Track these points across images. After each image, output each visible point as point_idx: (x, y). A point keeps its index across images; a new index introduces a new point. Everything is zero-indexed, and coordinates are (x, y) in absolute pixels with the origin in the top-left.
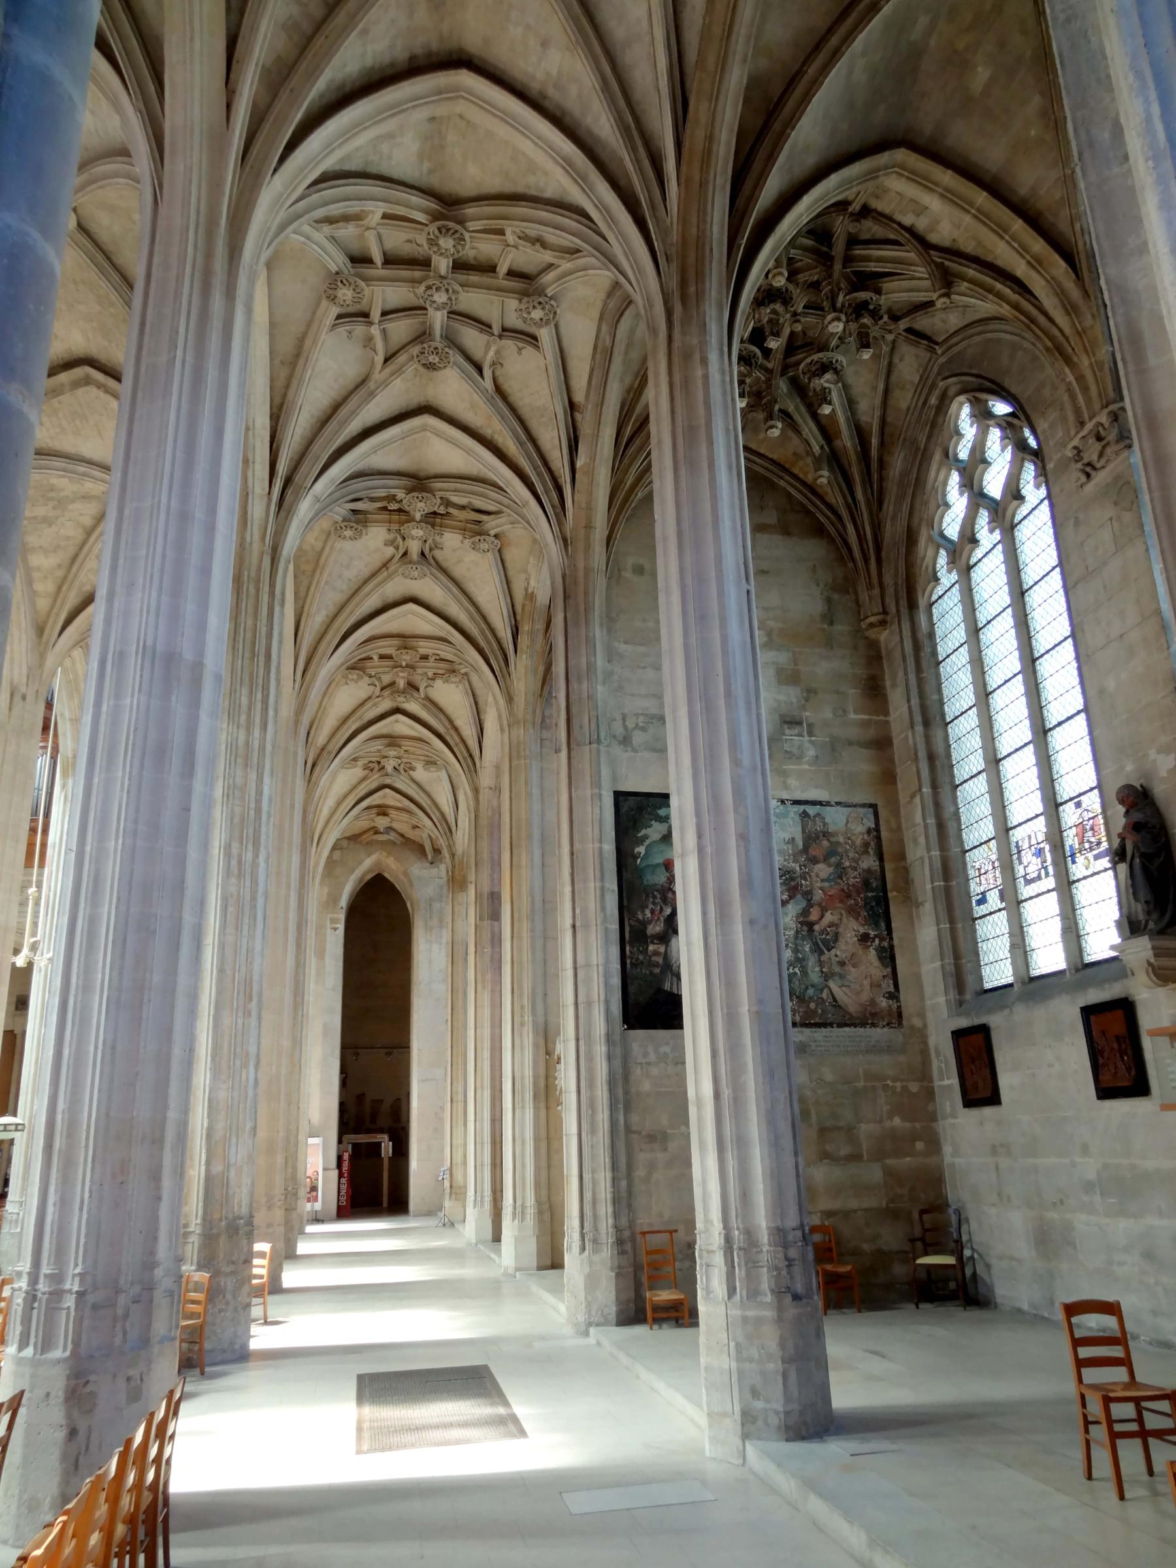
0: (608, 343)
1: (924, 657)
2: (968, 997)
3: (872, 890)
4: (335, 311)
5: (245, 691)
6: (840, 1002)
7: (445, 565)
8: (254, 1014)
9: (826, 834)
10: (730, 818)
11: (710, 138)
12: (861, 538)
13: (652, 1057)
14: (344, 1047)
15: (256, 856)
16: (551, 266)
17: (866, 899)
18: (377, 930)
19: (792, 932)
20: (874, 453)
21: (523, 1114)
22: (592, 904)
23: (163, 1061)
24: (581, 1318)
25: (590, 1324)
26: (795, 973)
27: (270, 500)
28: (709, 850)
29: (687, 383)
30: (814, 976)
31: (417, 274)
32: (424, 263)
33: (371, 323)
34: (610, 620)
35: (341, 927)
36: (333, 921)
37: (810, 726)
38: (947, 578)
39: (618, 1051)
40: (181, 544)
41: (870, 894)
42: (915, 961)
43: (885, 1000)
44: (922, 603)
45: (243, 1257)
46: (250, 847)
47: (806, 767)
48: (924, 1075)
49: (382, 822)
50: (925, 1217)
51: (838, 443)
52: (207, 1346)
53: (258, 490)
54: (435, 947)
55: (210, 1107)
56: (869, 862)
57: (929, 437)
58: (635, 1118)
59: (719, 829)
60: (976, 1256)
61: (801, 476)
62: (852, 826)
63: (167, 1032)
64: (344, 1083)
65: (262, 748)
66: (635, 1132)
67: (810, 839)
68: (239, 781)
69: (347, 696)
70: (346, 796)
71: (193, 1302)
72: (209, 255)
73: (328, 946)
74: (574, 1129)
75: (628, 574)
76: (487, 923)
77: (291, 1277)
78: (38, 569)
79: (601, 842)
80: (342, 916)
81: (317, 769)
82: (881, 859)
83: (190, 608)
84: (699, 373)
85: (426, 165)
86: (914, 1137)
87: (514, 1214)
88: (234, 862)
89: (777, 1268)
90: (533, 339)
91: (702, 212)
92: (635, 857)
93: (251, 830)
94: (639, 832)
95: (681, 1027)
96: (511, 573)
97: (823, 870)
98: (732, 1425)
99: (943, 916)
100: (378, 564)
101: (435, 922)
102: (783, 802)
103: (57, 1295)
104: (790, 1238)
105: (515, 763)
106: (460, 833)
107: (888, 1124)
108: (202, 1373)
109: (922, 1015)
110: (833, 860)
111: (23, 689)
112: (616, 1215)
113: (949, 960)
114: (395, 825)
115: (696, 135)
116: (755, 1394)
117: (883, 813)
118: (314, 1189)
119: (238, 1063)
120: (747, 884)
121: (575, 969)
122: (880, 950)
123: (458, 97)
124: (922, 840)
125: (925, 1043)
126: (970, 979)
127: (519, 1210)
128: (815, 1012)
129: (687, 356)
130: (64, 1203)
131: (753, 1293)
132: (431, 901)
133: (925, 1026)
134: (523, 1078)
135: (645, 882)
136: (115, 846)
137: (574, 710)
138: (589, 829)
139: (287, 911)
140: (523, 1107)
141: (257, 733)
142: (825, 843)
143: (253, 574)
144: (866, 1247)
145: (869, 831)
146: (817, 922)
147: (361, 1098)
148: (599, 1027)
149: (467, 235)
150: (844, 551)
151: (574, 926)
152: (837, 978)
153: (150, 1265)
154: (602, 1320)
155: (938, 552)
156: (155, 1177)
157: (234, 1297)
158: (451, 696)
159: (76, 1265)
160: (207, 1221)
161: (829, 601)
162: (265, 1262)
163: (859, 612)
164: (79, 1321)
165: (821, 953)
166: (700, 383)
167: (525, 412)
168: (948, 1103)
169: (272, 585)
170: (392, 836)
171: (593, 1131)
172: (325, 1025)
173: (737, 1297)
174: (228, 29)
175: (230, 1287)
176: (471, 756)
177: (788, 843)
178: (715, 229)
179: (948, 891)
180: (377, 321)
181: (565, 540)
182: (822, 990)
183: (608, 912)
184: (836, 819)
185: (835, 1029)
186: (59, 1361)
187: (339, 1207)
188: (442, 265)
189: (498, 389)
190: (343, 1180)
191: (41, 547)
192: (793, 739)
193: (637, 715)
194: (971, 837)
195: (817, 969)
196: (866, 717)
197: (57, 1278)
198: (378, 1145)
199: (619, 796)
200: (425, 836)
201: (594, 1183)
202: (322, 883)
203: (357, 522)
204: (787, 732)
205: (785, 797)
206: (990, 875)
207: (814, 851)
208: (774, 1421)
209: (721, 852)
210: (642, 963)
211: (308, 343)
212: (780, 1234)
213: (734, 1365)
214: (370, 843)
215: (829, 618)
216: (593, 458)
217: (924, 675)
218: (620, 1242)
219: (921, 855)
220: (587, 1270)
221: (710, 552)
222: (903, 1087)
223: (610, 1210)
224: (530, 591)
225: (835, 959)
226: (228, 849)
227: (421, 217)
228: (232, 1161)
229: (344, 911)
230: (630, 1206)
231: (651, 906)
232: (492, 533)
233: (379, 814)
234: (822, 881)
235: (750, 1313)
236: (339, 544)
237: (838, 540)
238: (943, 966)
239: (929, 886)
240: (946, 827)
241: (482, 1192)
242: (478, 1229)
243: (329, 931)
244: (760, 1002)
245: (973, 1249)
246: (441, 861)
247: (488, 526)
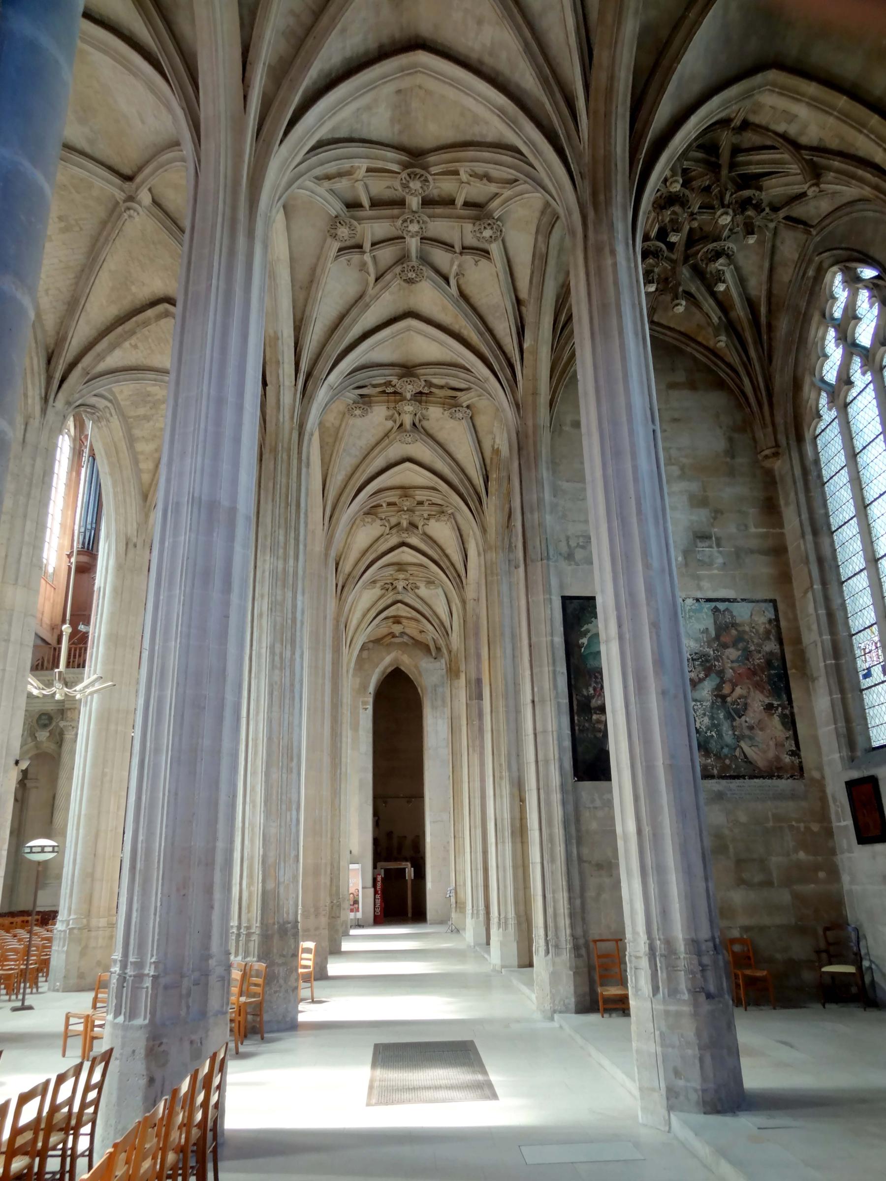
0: (544, 250)
1: (811, 479)
2: (859, 753)
3: (774, 669)
4: (336, 245)
5: (282, 532)
6: (750, 759)
7: (431, 432)
8: (295, 771)
9: (734, 625)
10: (644, 611)
11: (612, 78)
12: (756, 388)
13: (598, 803)
14: (376, 798)
15: (293, 653)
16: (496, 195)
17: (769, 677)
18: (397, 710)
19: (708, 704)
20: (763, 320)
21: (504, 845)
22: (547, 685)
23: (213, 803)
24: (548, 1006)
25: (555, 1012)
26: (712, 736)
27: (296, 390)
28: (627, 636)
29: (600, 270)
30: (728, 738)
31: (396, 212)
32: (400, 203)
33: (364, 252)
34: (554, 465)
35: (370, 707)
37: (718, 540)
38: (828, 415)
39: (571, 798)
40: (218, 422)
41: (772, 672)
42: (813, 724)
43: (788, 757)
44: (808, 437)
45: (291, 952)
46: (289, 647)
47: (716, 572)
48: (823, 815)
49: (397, 629)
50: (828, 933)
51: (733, 314)
52: (266, 1017)
53: (287, 383)
54: (440, 722)
55: (264, 840)
56: (771, 646)
57: (809, 302)
58: (585, 851)
59: (635, 618)
60: (873, 966)
61: (704, 342)
62: (756, 618)
64: (377, 824)
65: (295, 573)
66: (585, 862)
67: (721, 629)
68: (279, 598)
69: (365, 535)
70: (369, 610)
71: (256, 985)
72: (234, 208)
73: (361, 722)
74: (538, 859)
75: (567, 428)
76: (475, 702)
77: (335, 968)
78: (142, 453)
79: (552, 635)
80: (370, 700)
81: (346, 589)
82: (781, 642)
83: (225, 467)
84: (609, 262)
85: (397, 128)
86: (817, 868)
87: (499, 924)
88: (277, 658)
89: (692, 972)
90: (486, 253)
91: (608, 135)
92: (580, 647)
93: (289, 634)
94: (582, 627)
95: (608, 778)
96: (481, 435)
97: (733, 653)
98: (659, 1099)
99: (835, 688)
100: (381, 434)
101: (439, 702)
102: (698, 600)
103: (140, 977)
104: (704, 947)
105: (489, 578)
107: (794, 857)
108: (262, 1038)
109: (820, 768)
110: (741, 645)
111: (135, 540)
112: (572, 926)
113: (841, 724)
114: (408, 631)
115: (600, 77)
116: (677, 1073)
117: (780, 606)
118: (356, 902)
119: (284, 807)
120: (659, 662)
121: (535, 735)
122: (783, 717)
123: (416, 72)
124: (815, 627)
125: (823, 791)
126: (860, 740)
127: (502, 921)
128: (729, 767)
129: (599, 250)
130: (144, 909)
131: (673, 992)
132: (436, 686)
133: (823, 777)
134: (502, 820)
135: (588, 666)
136: (174, 646)
137: (528, 535)
138: (543, 626)
139: (323, 695)
140: (503, 842)
141: (291, 562)
142: (734, 632)
143: (285, 445)
144: (778, 956)
145: (770, 621)
146: (729, 695)
148: (555, 779)
149: (430, 178)
150: (742, 400)
151: (533, 702)
152: (747, 739)
154: (563, 1008)
155: (819, 395)
156: (209, 890)
157: (285, 982)
158: (442, 531)
159: (152, 956)
160: (264, 925)
161: (731, 440)
162: (311, 956)
163: (756, 447)
164: (154, 997)
165: (734, 720)
166: (610, 270)
167: (483, 310)
168: (845, 841)
169: (300, 453)
170: (405, 639)
171: (553, 860)
173: (660, 995)
174: (242, 43)
175: (282, 974)
176: (459, 576)
177: (703, 632)
178: (619, 150)
179: (838, 668)
180: (368, 250)
181: (517, 406)
182: (735, 749)
183: (560, 690)
184: (742, 613)
185: (747, 781)
186: (141, 1027)
187: (375, 917)
188: (414, 202)
189: (463, 295)
190: (378, 896)
191: (143, 437)
192: (705, 550)
193: (578, 537)
194: (856, 624)
195: (730, 732)
196: (765, 530)
197: (139, 965)
199: (566, 600)
200: (429, 638)
201: (555, 901)
202: (354, 675)
203: (364, 403)
204: (699, 544)
205: (699, 595)
206: (874, 654)
207: (724, 639)
208: (694, 1097)
209: (637, 637)
210: (588, 729)
211: (318, 271)
212: (694, 944)
213: (659, 1049)
214: (390, 645)
215: (731, 453)
216: (536, 340)
217: (812, 494)
218: (576, 948)
219: (814, 639)
220: (551, 969)
221: (622, 400)
222: (805, 827)
223: (568, 922)
224: (496, 447)
225: (745, 725)
226: (272, 648)
227: (395, 167)
228: (282, 880)
229: (372, 696)
230: (583, 919)
231: (593, 685)
232: (465, 404)
234: (732, 662)
235: (672, 1008)
236: (352, 421)
237: (737, 391)
238: (836, 729)
239: (822, 664)
240: (835, 617)
241: (478, 906)
243: (361, 711)
244: (673, 757)
245: (871, 961)
246: (442, 657)
247: (462, 400)
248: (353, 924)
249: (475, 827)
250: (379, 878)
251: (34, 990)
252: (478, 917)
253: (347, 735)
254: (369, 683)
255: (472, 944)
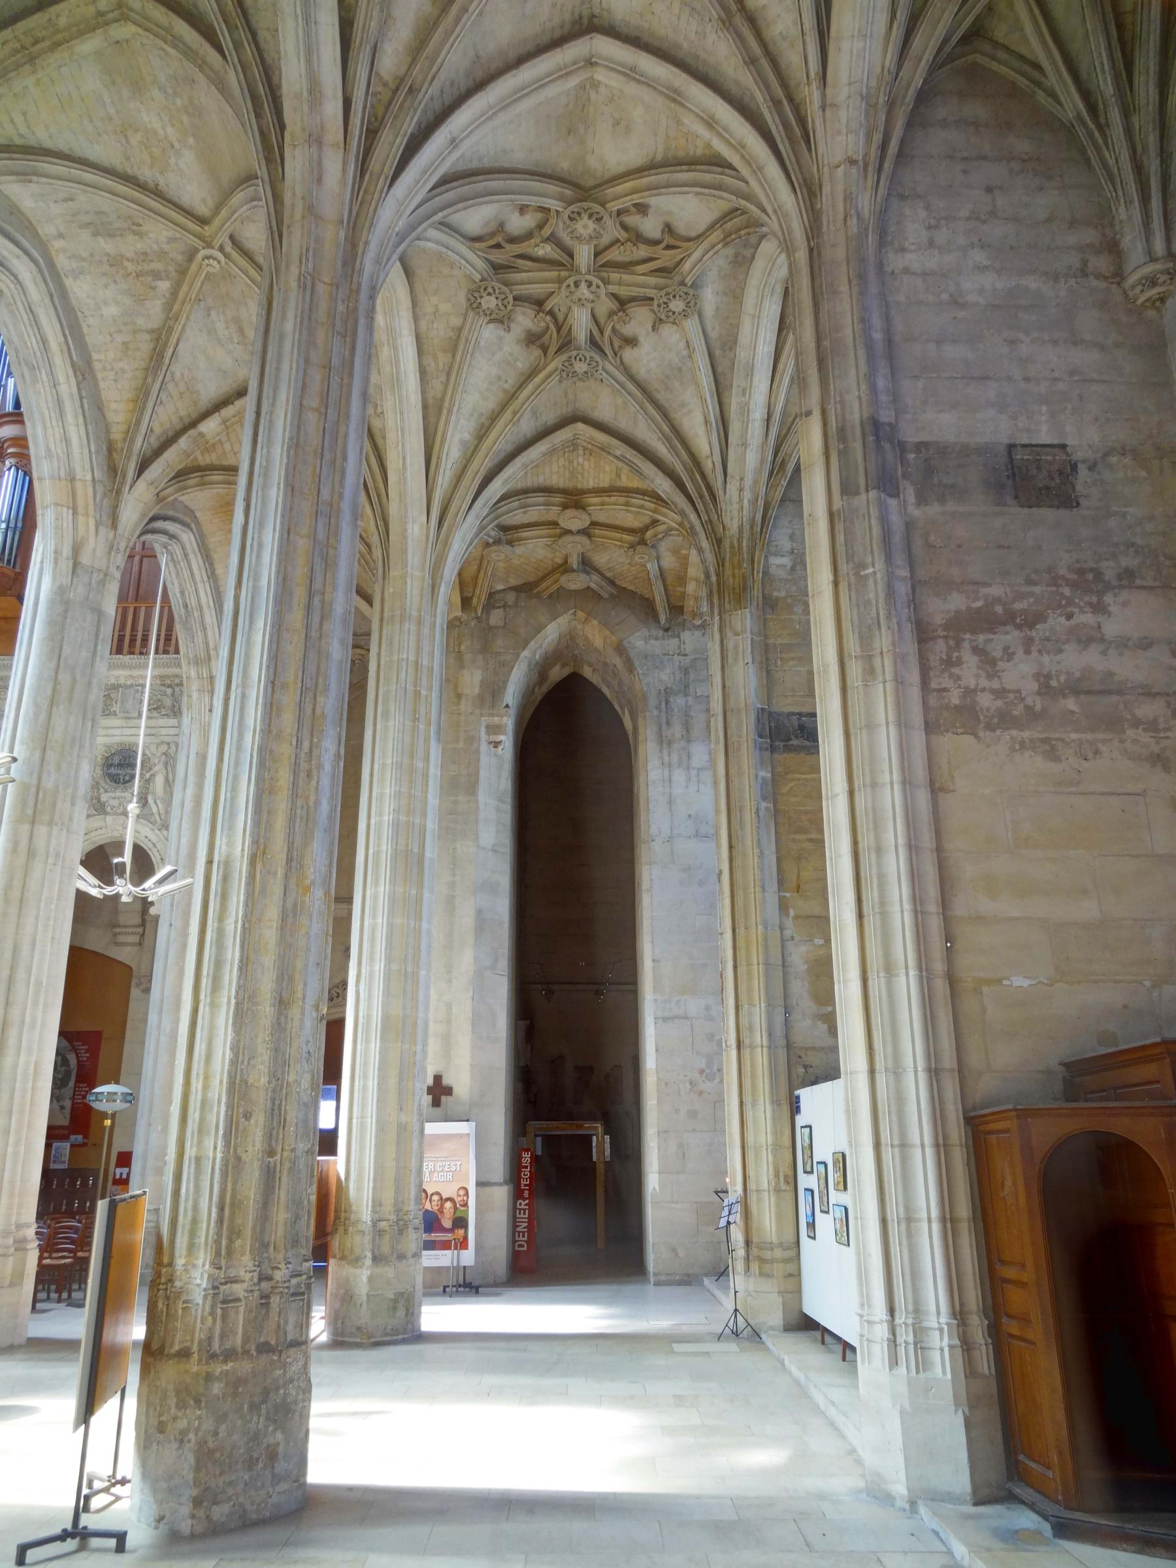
35: (507, 741)
36: (493, 729)
54: (679, 776)
73: (483, 774)
76: (867, 500)
101: (677, 730)
106: (733, 488)
114: (601, 559)
118: (460, 1222)
132: (668, 692)
172: (479, 912)
198: (587, 1139)
229: (512, 712)
233: (565, 507)
241: (918, 1311)
242: (917, 1451)
243: (484, 747)
246: (683, 625)
248: (451, 1281)
249: (889, 969)
251: (65, 1295)
252: (922, 1364)
254: (505, 682)
255: (900, 1489)
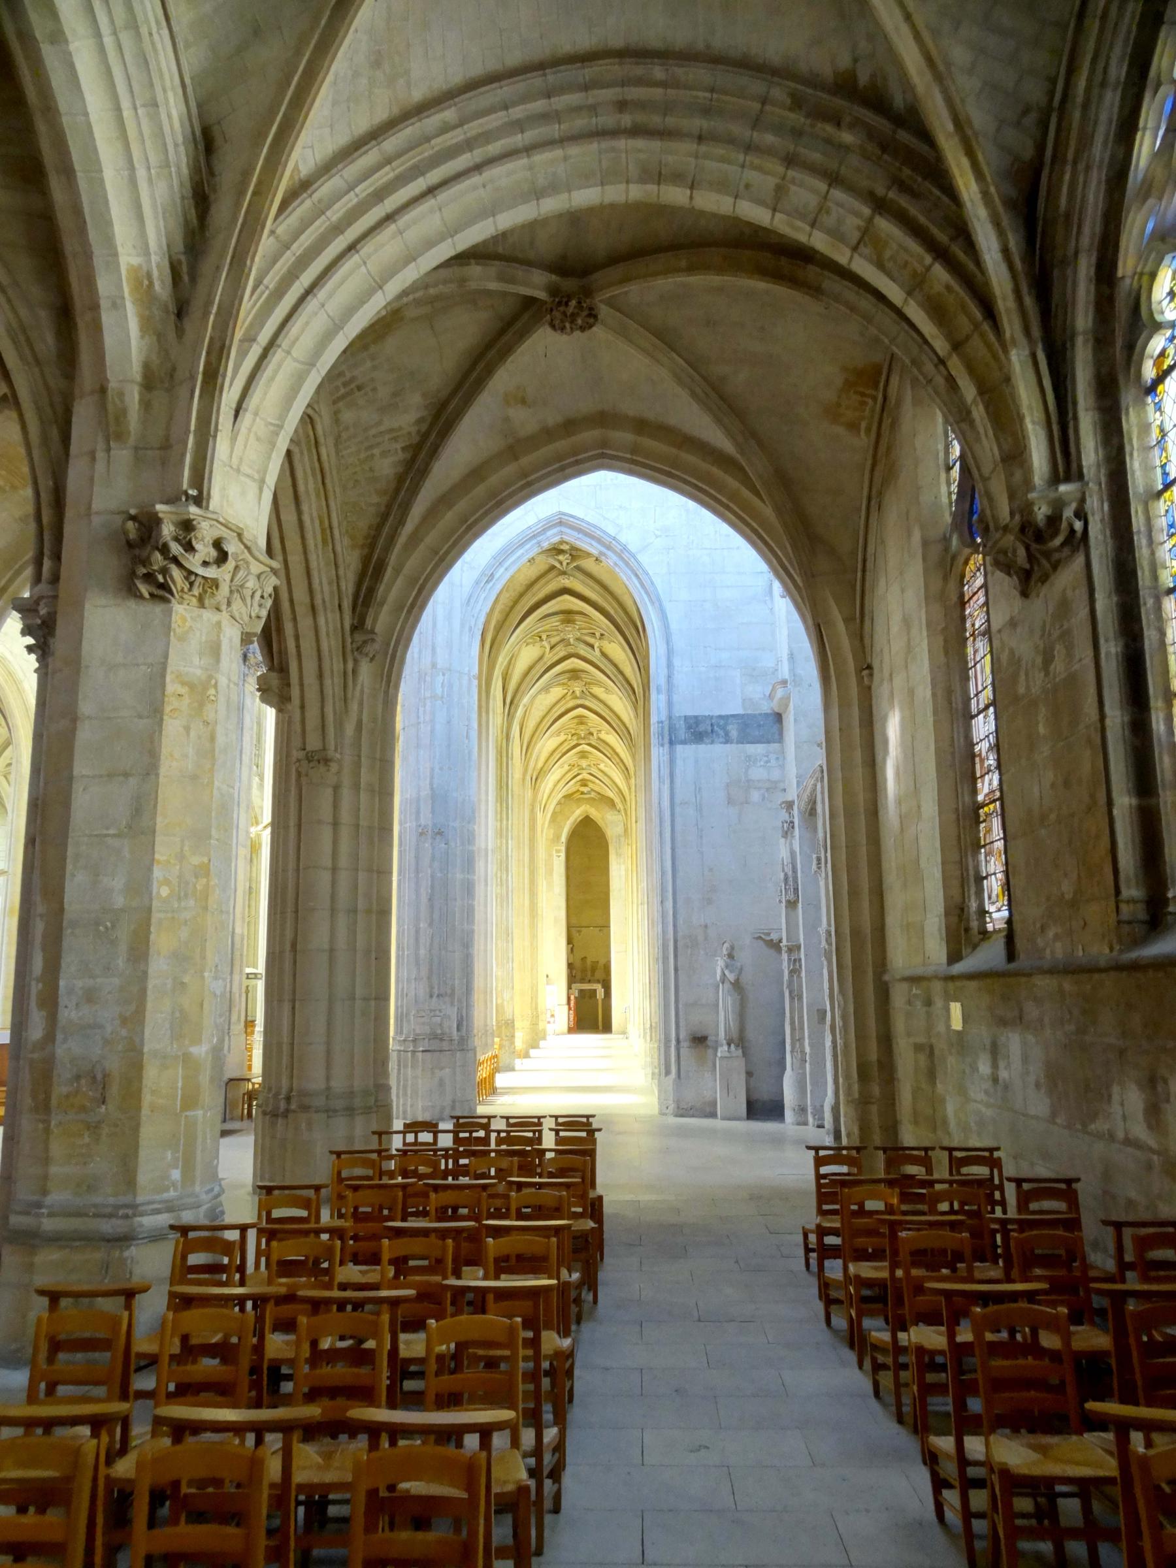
35: (563, 855)
36: (558, 851)
49: (585, 789)
63: (486, 963)
80: (563, 848)
98: (650, 1076)
147: (584, 959)
153: (486, 1025)
250: (572, 997)
253: (542, 885)
